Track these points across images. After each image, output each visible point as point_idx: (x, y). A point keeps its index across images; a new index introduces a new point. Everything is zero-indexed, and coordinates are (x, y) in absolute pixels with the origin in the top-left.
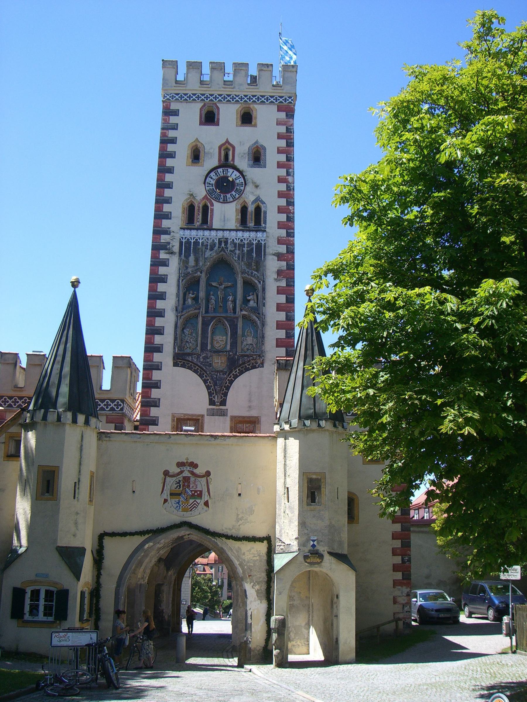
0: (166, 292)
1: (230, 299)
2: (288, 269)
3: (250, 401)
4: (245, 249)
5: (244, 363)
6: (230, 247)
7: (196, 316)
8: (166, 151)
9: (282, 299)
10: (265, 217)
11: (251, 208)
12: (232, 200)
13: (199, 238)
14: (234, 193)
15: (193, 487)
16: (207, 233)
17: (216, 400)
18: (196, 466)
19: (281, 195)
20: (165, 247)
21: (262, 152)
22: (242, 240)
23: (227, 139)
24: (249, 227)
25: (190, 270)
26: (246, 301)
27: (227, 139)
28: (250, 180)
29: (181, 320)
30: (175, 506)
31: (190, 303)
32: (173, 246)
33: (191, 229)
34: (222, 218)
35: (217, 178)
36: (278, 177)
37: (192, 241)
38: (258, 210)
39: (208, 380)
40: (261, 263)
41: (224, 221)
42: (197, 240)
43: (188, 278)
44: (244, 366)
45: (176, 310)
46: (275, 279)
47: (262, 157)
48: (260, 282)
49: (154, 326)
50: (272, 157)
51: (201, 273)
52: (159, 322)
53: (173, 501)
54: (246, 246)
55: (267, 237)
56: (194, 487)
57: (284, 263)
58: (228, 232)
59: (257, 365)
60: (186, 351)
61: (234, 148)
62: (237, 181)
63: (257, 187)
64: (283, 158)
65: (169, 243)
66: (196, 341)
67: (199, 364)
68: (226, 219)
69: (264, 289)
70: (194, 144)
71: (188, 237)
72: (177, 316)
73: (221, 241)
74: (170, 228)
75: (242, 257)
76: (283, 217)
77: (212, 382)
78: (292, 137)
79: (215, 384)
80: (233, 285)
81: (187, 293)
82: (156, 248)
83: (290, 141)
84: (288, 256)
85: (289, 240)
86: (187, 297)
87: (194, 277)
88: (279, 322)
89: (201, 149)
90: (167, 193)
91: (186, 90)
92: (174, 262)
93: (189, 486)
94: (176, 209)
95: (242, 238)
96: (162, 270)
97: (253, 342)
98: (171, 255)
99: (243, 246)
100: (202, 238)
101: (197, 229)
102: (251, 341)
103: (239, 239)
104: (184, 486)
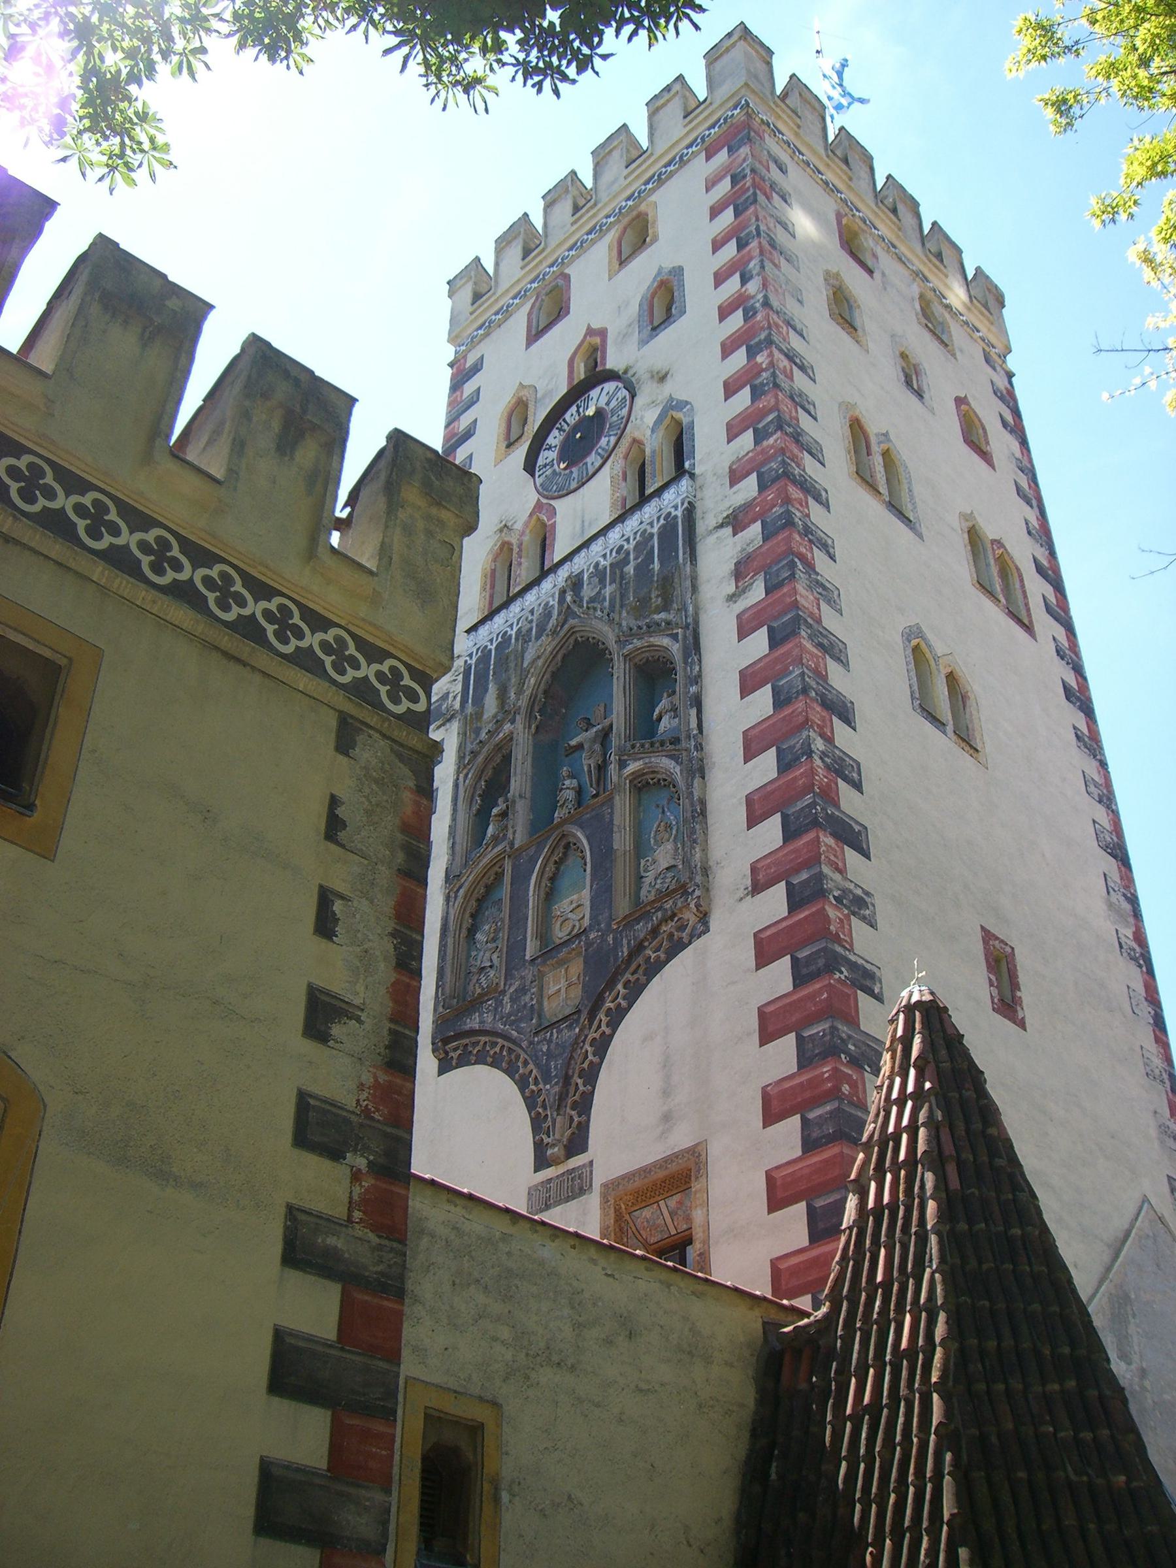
3: (666, 1093)
5: (639, 948)
44: (640, 960)
51: (513, 722)
59: (685, 935)
91: (497, 301)
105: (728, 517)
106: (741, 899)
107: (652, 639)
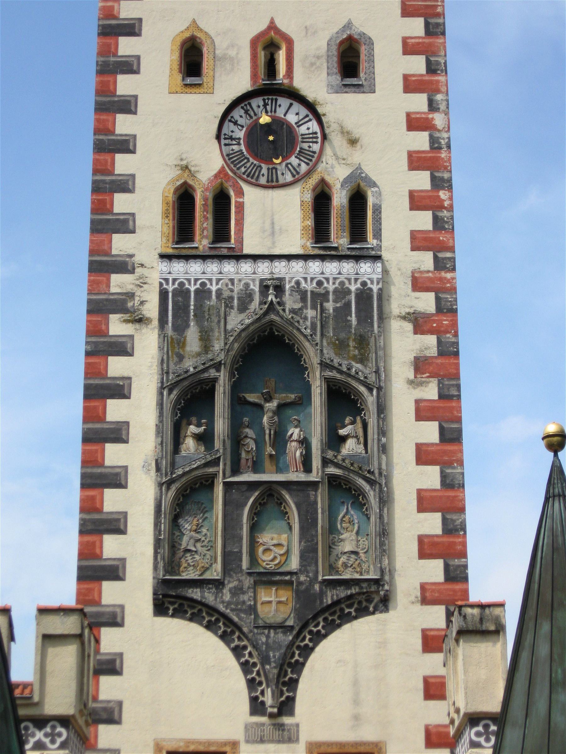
0: (127, 423)
1: (295, 437)
2: (442, 353)
3: (356, 702)
4: (330, 306)
6: (291, 301)
7: (208, 483)
8: (115, 54)
9: (430, 432)
10: (378, 220)
11: (340, 199)
12: (289, 178)
13: (210, 280)
14: (294, 160)
16: (229, 267)
17: (268, 699)
19: (416, 161)
20: (121, 305)
21: (363, 51)
22: (320, 283)
23: (272, 22)
24: (336, 249)
25: (189, 365)
26: (335, 441)
27: (272, 22)
28: (334, 126)
29: (172, 493)
31: (192, 450)
32: (142, 303)
33: (187, 258)
34: (267, 226)
35: (249, 122)
36: (408, 115)
37: (193, 289)
38: (358, 200)
39: (245, 648)
40: (372, 340)
41: (273, 233)
42: (203, 284)
43: (186, 383)
44: (337, 608)
45: (158, 469)
46: (411, 382)
47: (363, 66)
48: (370, 390)
49: (99, 510)
50: (389, 64)
51: (218, 370)
52: (112, 500)
54: (331, 297)
55: (385, 271)
57: (431, 340)
58: (284, 263)
60: (185, 576)
61: (290, 42)
62: (303, 130)
63: (353, 142)
64: (417, 65)
65: (131, 295)
66: (211, 547)
67: (221, 608)
68: (277, 228)
69: (382, 409)
70: (187, 35)
71: (182, 278)
72: (161, 485)
73: (267, 287)
74: (131, 256)
75: (322, 327)
76: (424, 221)
77: (255, 653)
78: (439, 10)
79: (265, 660)
80: (300, 398)
81: (184, 422)
82: (101, 307)
83: (433, 21)
84: (441, 322)
85: (441, 279)
86: (182, 435)
87: (201, 382)
88: (423, 494)
89: (205, 50)
90: (123, 164)
92: (148, 344)
94: (147, 207)
95: (320, 277)
96: (116, 366)
97: (357, 546)
98: (137, 326)
99: (324, 296)
100: (218, 281)
101: (204, 258)
102: (354, 543)
103: (312, 279)
105: (409, 313)
106: (413, 603)
107: (349, 379)
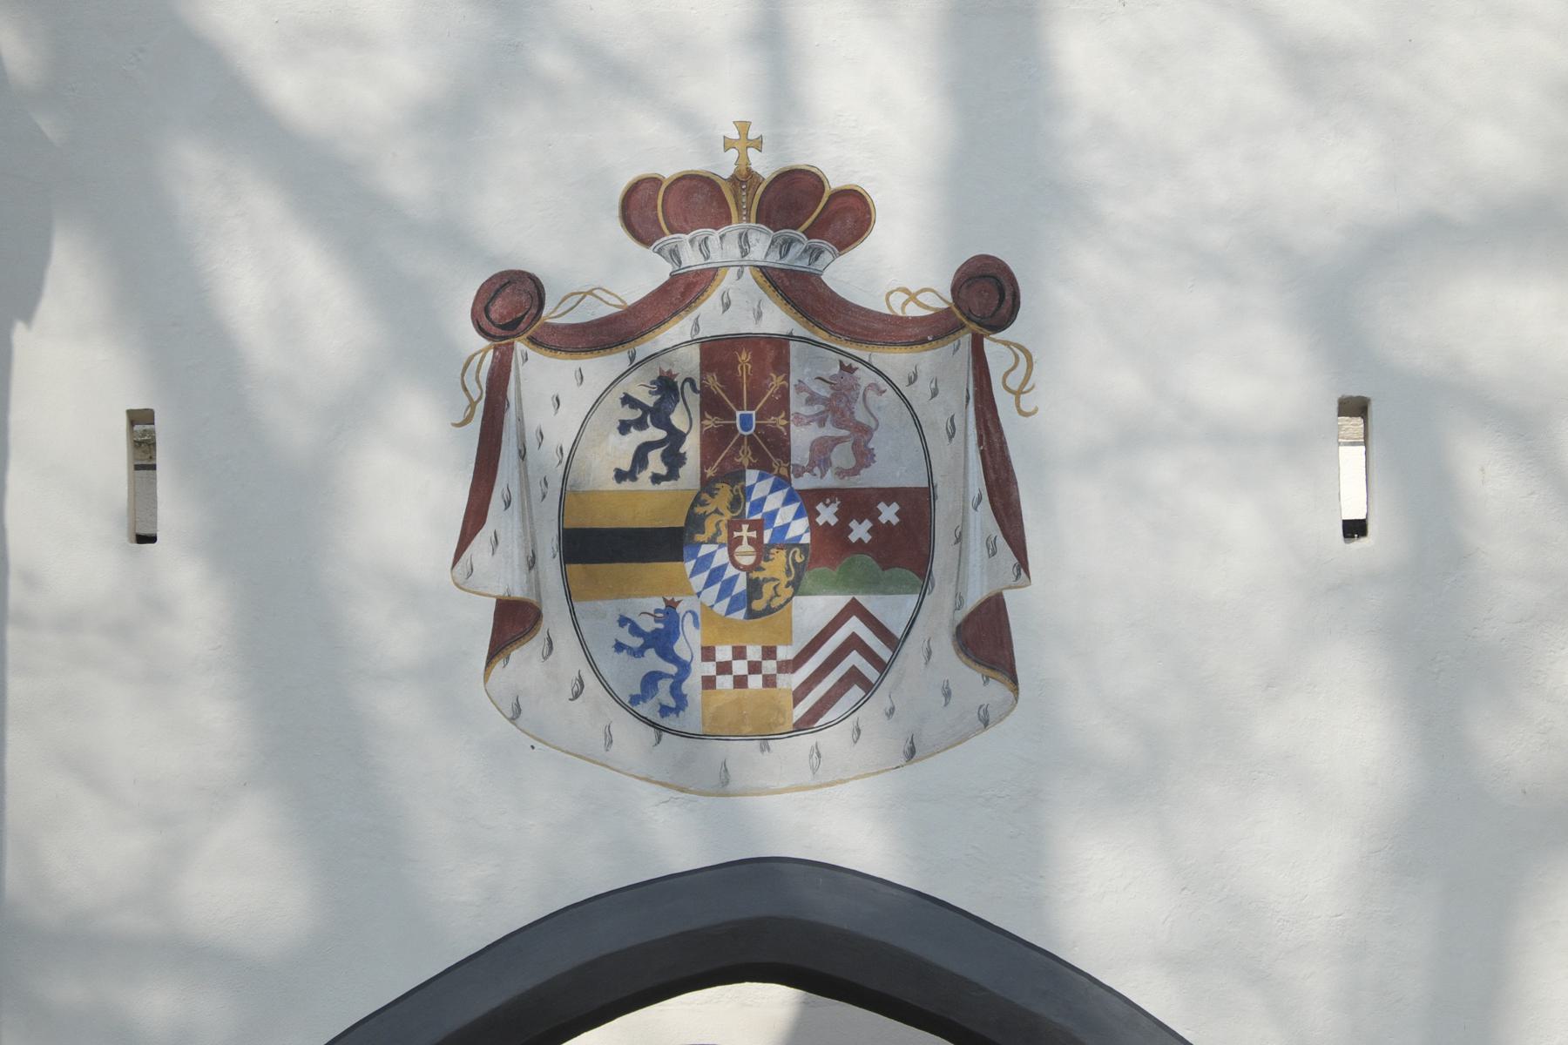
15: (821, 454)
18: (848, 217)
30: (627, 673)
53: (601, 616)
56: (842, 456)
93: (771, 450)
104: (714, 442)
